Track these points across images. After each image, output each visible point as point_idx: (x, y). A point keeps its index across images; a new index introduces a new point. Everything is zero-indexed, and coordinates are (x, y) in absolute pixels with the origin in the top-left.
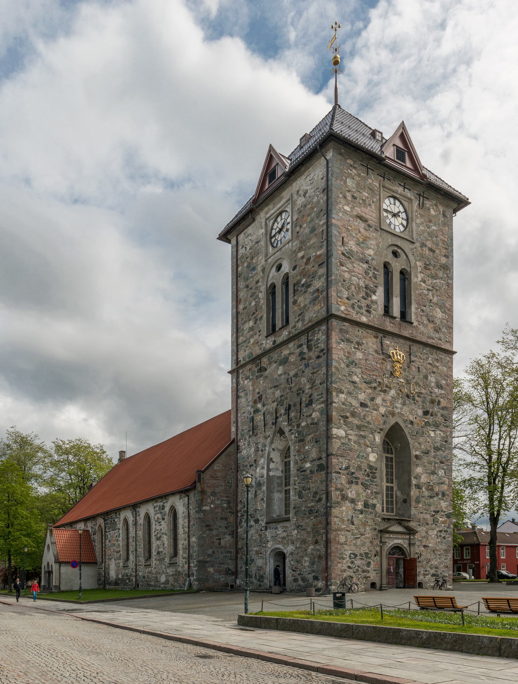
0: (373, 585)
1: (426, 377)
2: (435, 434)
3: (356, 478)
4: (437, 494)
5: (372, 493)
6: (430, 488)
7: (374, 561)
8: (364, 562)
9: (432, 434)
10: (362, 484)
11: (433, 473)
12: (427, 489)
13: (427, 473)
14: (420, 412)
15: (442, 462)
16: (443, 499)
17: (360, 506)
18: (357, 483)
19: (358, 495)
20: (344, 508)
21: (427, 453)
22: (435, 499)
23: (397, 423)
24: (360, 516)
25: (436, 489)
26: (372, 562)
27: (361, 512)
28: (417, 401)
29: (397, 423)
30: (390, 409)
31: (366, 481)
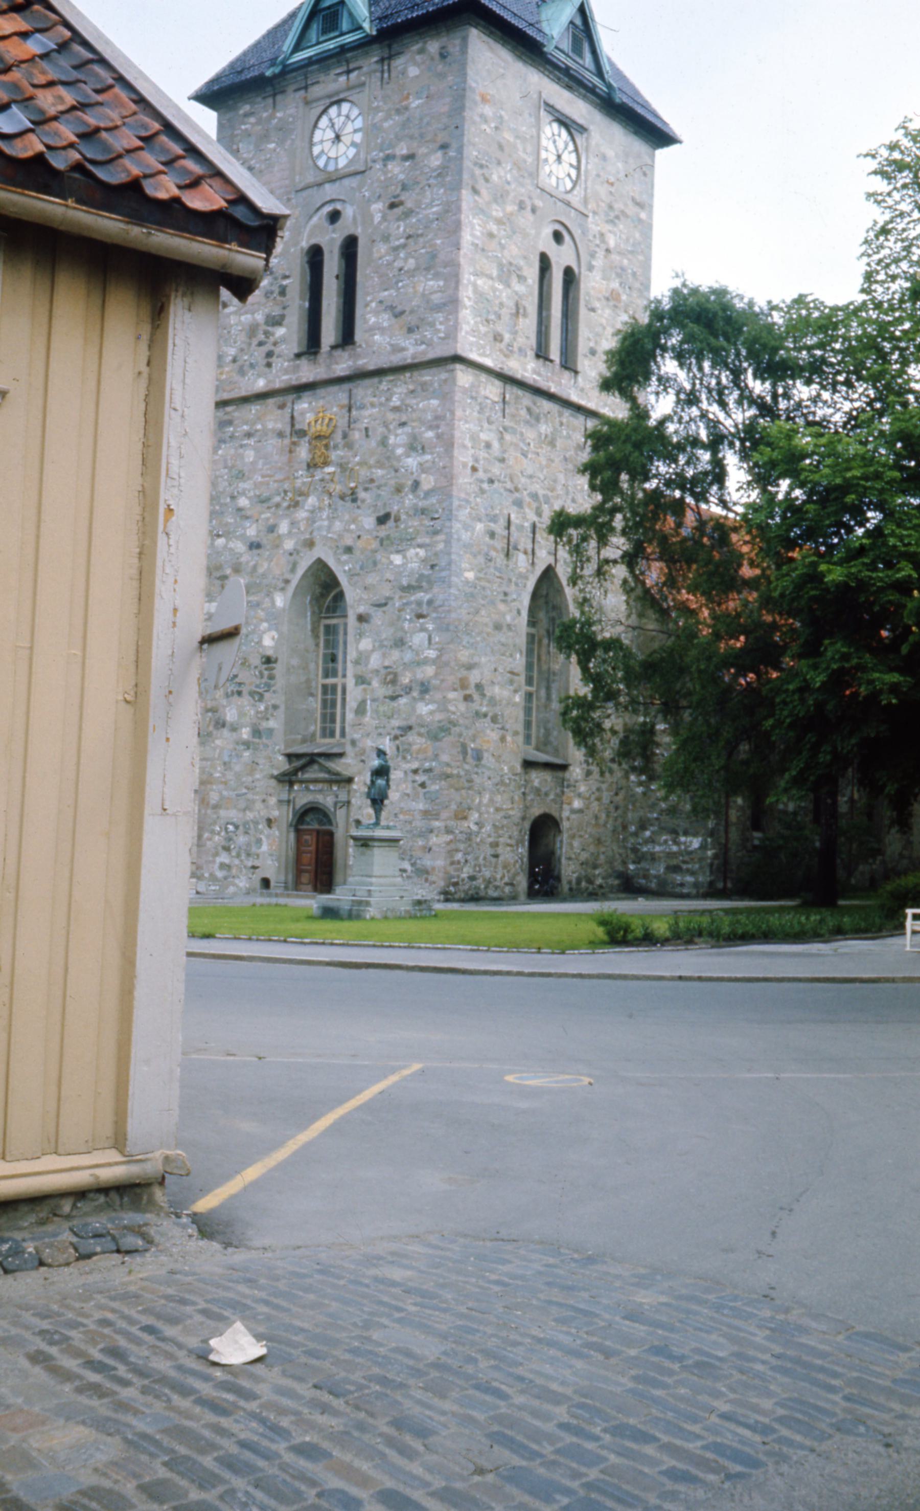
0: (266, 883)
1: (384, 442)
2: (405, 557)
3: (240, 684)
4: (408, 690)
5: (267, 709)
6: (391, 678)
7: (268, 837)
8: (253, 839)
9: (397, 559)
10: (252, 694)
11: (400, 643)
12: (385, 682)
13: (382, 646)
14: (369, 522)
15: (420, 616)
16: (422, 699)
17: (245, 734)
18: (239, 693)
19: (241, 714)
20: (218, 742)
21: (386, 604)
22: (403, 701)
23: (319, 561)
24: (246, 754)
25: (405, 680)
26: (264, 839)
27: (247, 745)
28: (363, 501)
29: (319, 561)
30: (308, 536)
31: (257, 686)
